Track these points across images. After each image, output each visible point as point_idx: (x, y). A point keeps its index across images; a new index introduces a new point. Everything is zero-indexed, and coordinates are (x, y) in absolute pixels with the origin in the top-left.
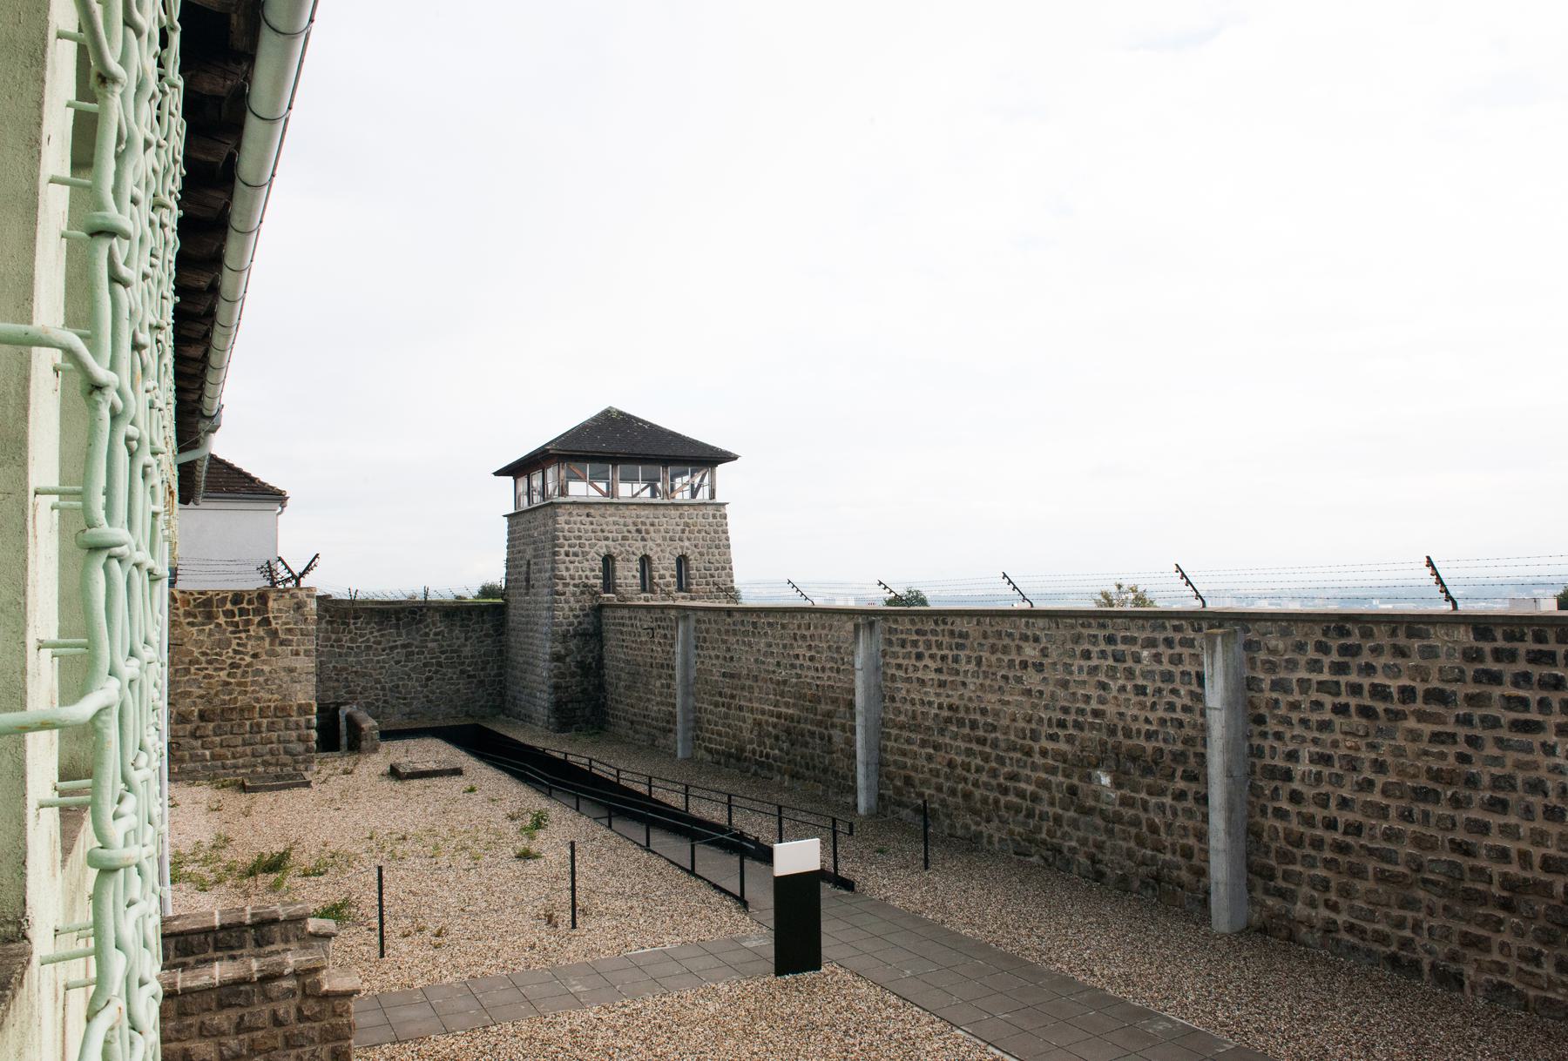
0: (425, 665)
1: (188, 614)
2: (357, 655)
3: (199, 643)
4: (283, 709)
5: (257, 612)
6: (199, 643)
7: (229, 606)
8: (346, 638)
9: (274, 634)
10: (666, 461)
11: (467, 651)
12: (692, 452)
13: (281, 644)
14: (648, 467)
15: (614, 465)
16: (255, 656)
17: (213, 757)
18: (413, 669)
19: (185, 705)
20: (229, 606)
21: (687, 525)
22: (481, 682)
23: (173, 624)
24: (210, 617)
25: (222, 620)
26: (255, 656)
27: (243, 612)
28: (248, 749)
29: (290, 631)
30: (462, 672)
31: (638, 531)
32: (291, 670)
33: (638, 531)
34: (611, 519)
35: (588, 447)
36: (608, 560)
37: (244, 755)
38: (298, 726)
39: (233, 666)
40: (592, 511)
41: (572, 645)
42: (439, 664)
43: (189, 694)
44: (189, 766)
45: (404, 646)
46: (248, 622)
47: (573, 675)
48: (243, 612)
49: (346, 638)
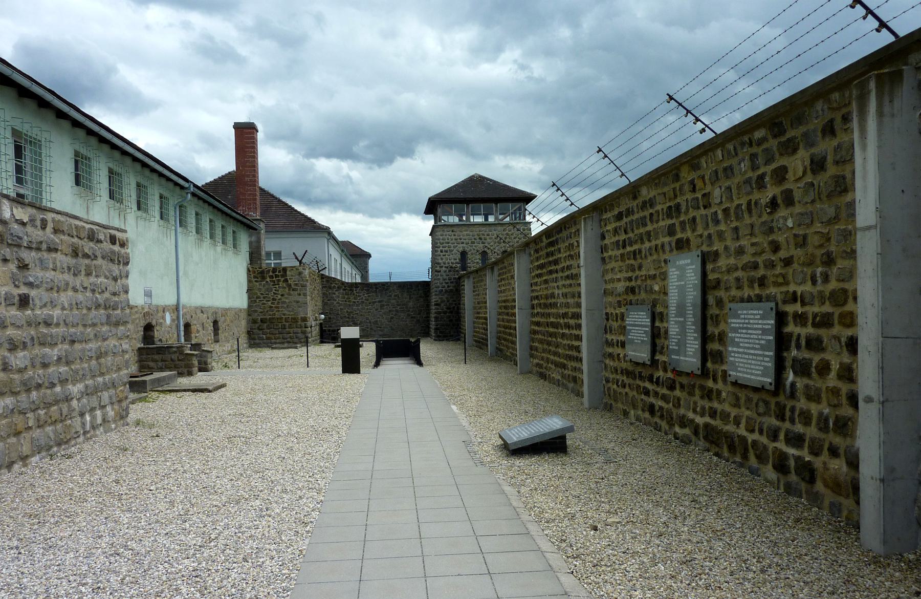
0: (390, 311)
1: (255, 277)
2: (357, 305)
3: (260, 290)
4: (294, 319)
5: (282, 276)
6: (260, 290)
7: (271, 274)
8: (352, 297)
9: (290, 286)
10: (497, 201)
11: (411, 304)
12: (510, 195)
13: (293, 290)
14: (458, 205)
15: (468, 205)
16: (282, 295)
17: (268, 338)
18: (384, 314)
19: (255, 316)
20: (271, 274)
21: (507, 234)
22: (418, 321)
23: (249, 281)
24: (263, 278)
25: (268, 279)
26: (282, 295)
27: (277, 276)
28: (281, 336)
29: (296, 285)
30: (409, 315)
31: (480, 239)
32: (298, 302)
33: (480, 239)
34: (465, 234)
35: (462, 195)
36: (464, 254)
37: (279, 338)
38: (301, 327)
39: (274, 299)
40: (455, 229)
41: (444, 298)
42: (397, 311)
43: (256, 311)
44: (257, 341)
45: (379, 302)
46: (279, 281)
47: (445, 313)
48: (277, 276)
49: (352, 297)
